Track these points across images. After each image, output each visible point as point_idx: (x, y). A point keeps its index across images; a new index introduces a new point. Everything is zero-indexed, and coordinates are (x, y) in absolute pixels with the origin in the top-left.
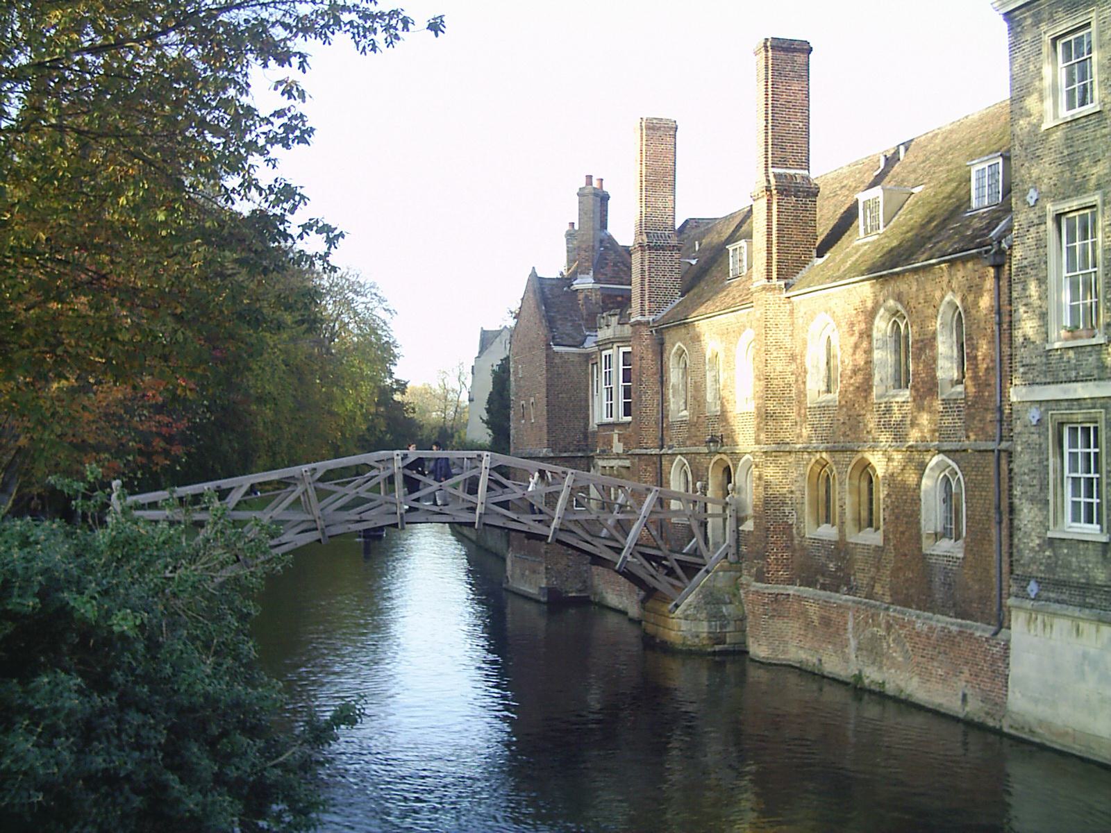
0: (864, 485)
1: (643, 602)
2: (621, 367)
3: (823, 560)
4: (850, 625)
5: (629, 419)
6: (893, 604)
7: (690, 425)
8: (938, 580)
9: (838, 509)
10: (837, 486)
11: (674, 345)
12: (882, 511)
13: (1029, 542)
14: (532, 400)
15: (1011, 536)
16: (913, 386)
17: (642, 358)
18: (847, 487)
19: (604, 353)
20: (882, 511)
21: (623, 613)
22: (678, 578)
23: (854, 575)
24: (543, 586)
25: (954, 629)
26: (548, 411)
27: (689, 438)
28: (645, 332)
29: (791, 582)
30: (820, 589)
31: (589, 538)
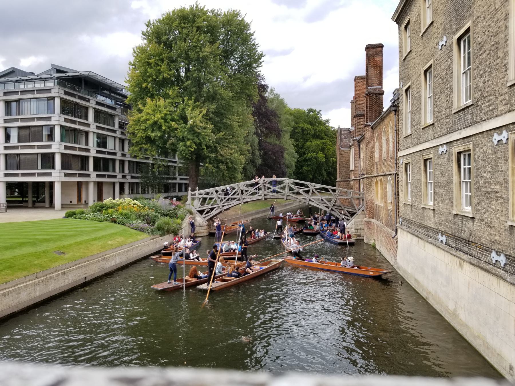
7: (363, 169)
13: (401, 205)
15: (398, 203)
28: (356, 142)
29: (373, 218)
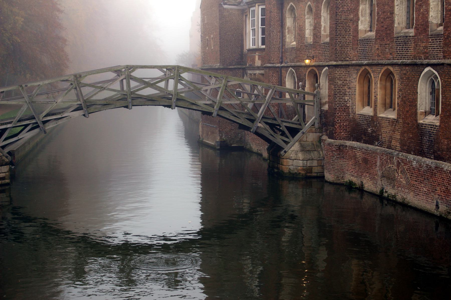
0: (388, 84)
1: (268, 149)
2: (260, 17)
3: (365, 127)
4: (378, 164)
5: (264, 47)
6: (401, 151)
8: (426, 139)
9: (373, 98)
10: (373, 85)
11: (288, 4)
12: (397, 99)
14: (212, 36)
16: (416, 27)
17: (271, 12)
18: (379, 85)
19: (252, 9)
20: (397, 99)
21: (261, 155)
22: (287, 137)
23: (381, 135)
24: (218, 140)
25: (433, 166)
26: (220, 42)
27: (296, 58)
30: (363, 143)
31: (236, 115)
